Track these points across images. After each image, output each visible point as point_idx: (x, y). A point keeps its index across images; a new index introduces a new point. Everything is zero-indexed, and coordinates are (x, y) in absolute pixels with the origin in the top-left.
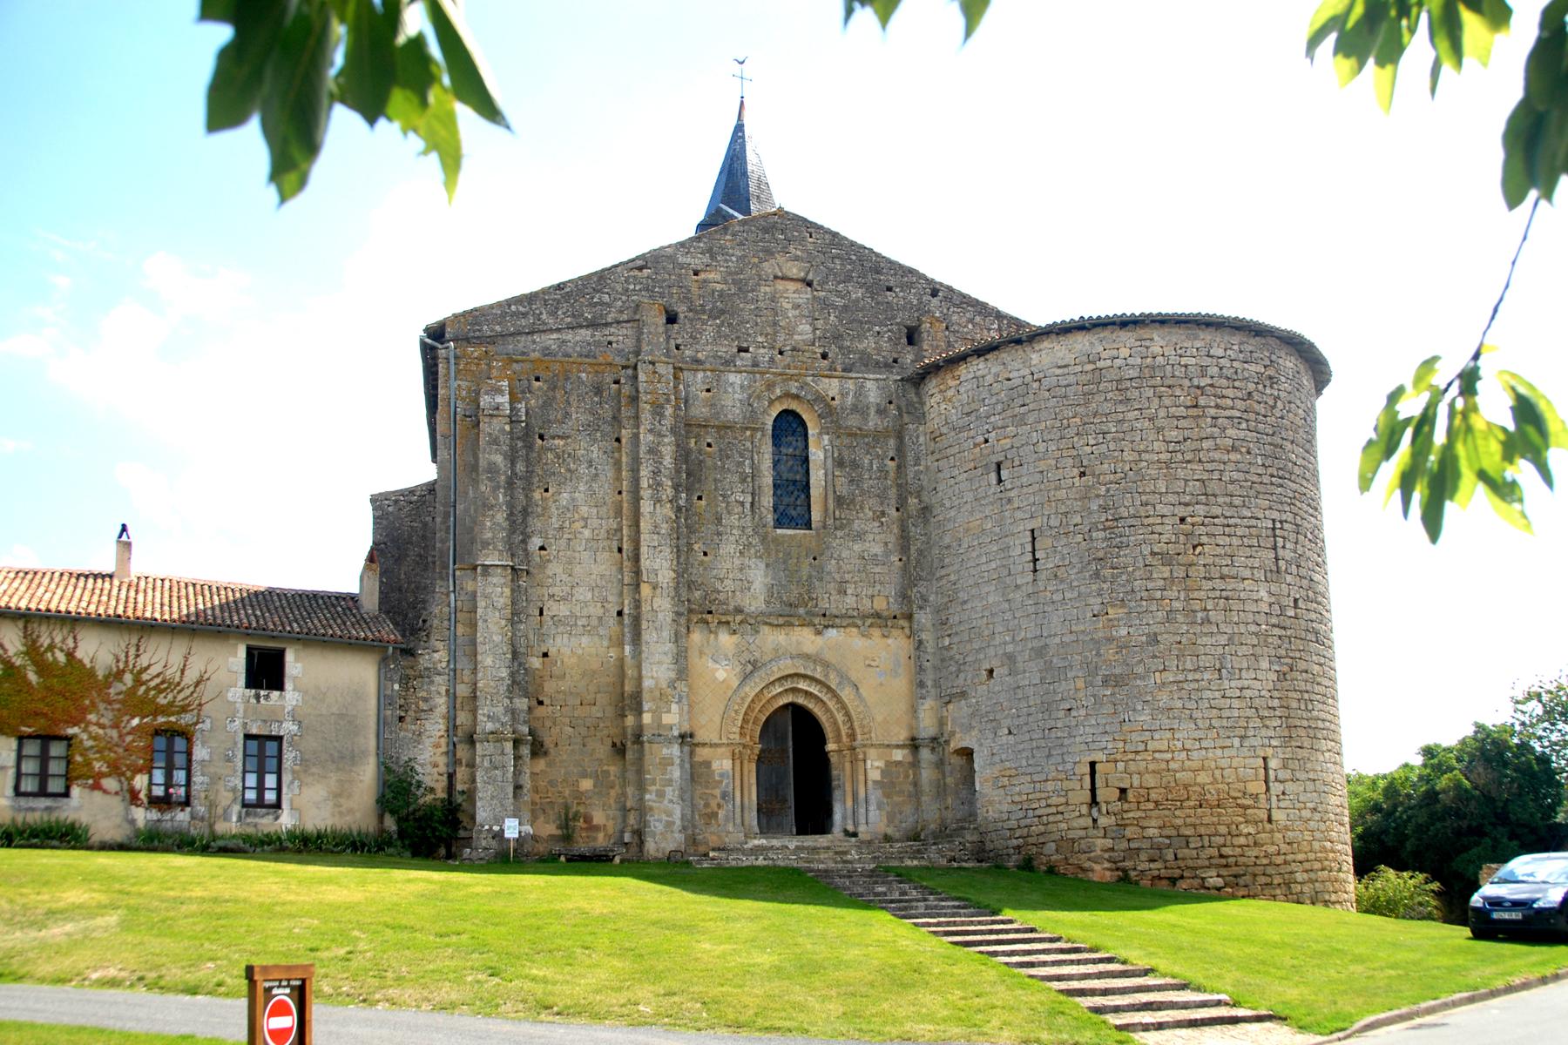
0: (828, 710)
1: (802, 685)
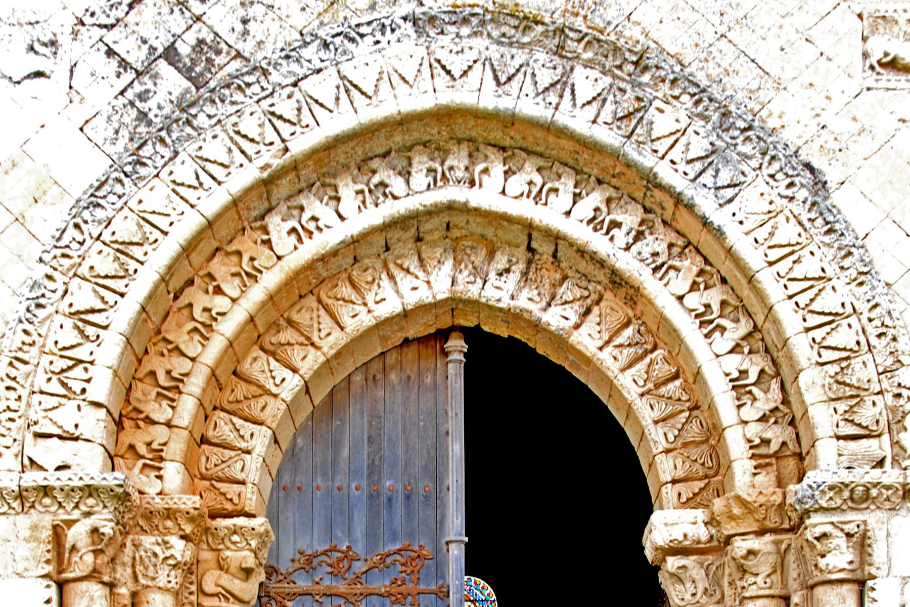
0: (656, 335)
1: (497, 190)
